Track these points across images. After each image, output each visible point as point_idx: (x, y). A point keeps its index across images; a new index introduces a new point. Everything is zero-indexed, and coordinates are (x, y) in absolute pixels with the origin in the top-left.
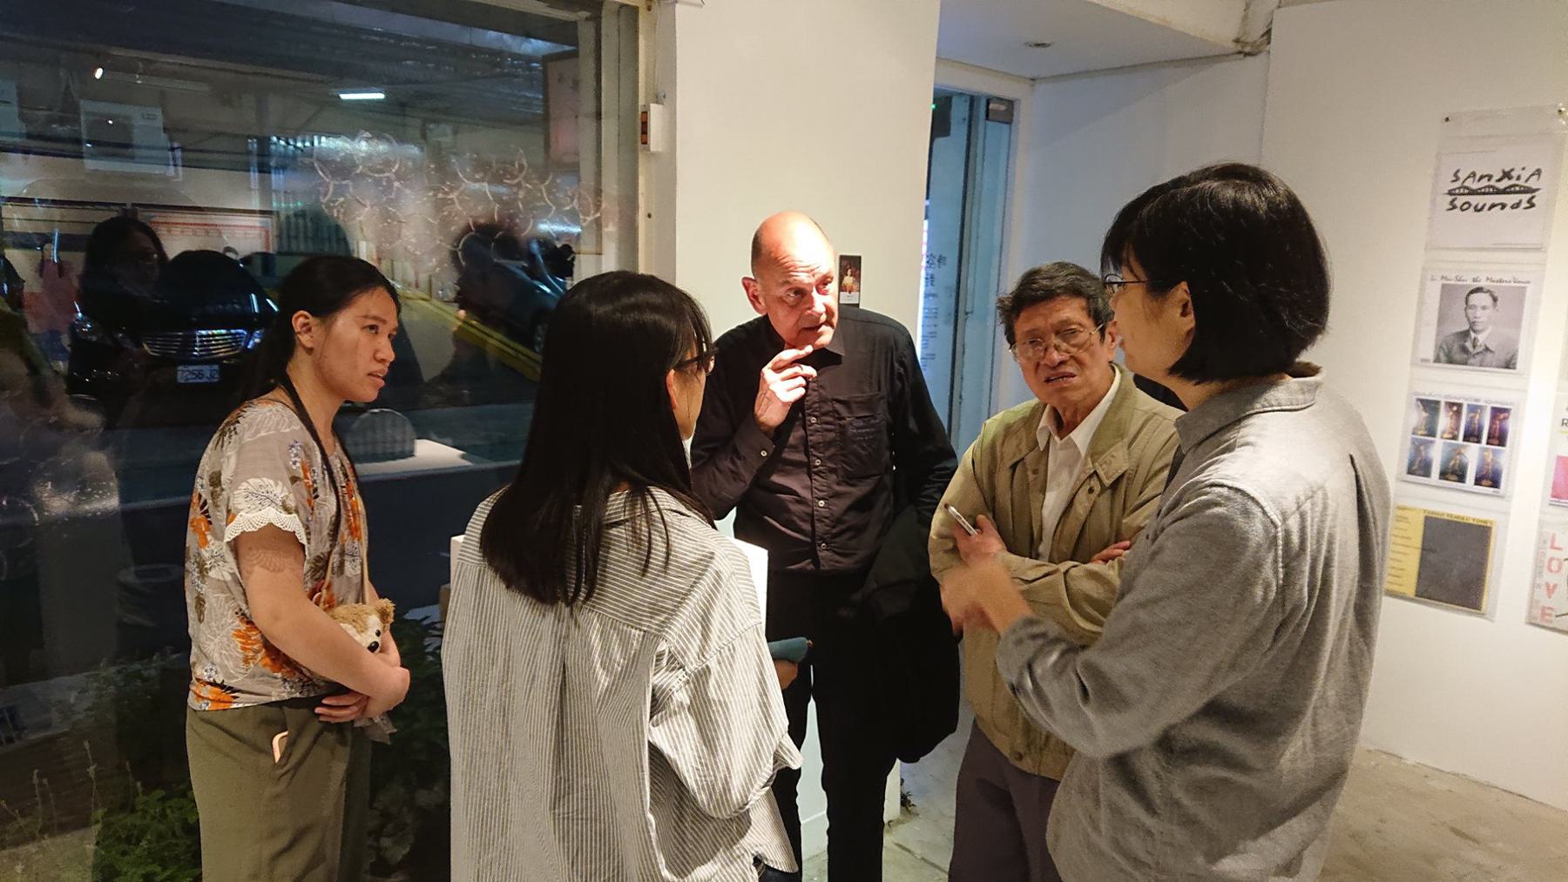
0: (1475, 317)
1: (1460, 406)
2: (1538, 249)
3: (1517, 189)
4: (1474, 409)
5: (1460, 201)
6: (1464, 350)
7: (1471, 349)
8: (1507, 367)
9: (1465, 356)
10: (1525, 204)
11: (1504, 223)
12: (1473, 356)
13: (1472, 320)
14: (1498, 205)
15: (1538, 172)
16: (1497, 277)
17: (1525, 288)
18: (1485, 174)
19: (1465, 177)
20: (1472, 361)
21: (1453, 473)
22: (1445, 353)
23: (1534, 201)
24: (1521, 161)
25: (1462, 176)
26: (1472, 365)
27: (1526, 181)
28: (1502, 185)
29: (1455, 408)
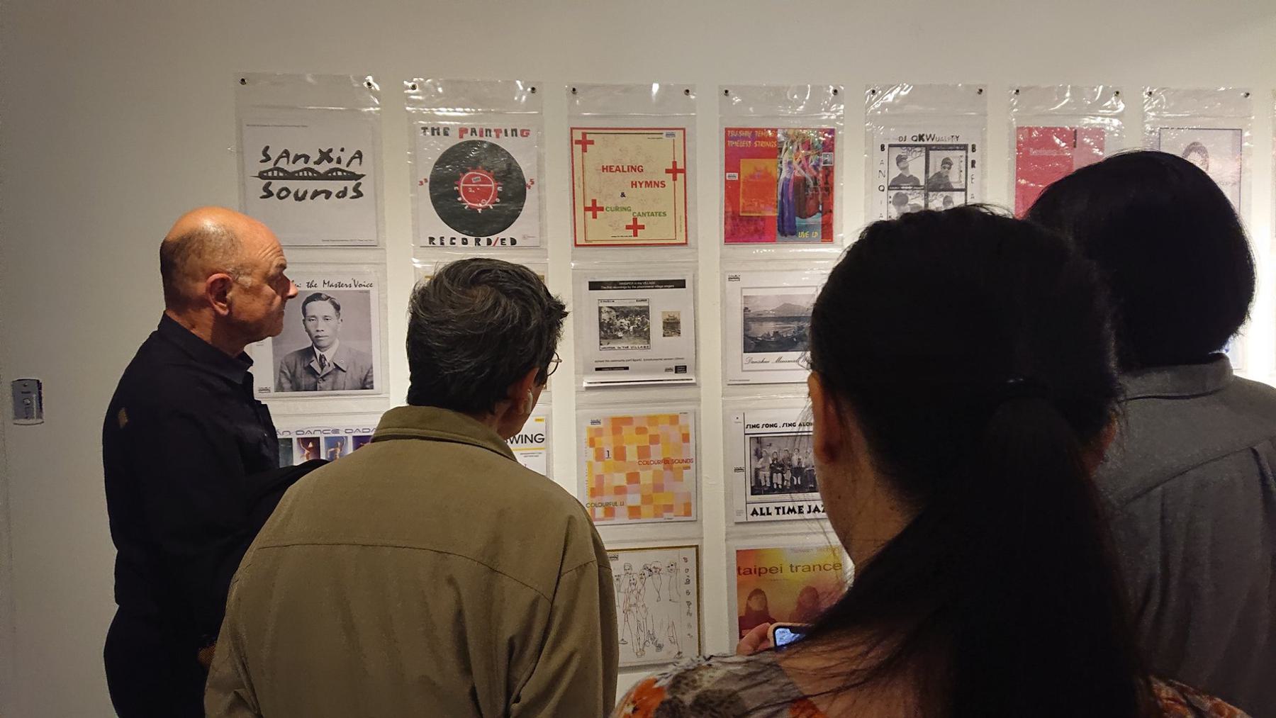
2: (373, 246)
3: (340, 173)
5: (276, 186)
6: (312, 372)
7: (319, 370)
9: (313, 380)
10: (351, 193)
12: (321, 378)
15: (359, 155)
17: (368, 292)
19: (276, 158)
20: (322, 384)
22: (288, 379)
24: (342, 142)
27: (348, 166)
28: (324, 167)
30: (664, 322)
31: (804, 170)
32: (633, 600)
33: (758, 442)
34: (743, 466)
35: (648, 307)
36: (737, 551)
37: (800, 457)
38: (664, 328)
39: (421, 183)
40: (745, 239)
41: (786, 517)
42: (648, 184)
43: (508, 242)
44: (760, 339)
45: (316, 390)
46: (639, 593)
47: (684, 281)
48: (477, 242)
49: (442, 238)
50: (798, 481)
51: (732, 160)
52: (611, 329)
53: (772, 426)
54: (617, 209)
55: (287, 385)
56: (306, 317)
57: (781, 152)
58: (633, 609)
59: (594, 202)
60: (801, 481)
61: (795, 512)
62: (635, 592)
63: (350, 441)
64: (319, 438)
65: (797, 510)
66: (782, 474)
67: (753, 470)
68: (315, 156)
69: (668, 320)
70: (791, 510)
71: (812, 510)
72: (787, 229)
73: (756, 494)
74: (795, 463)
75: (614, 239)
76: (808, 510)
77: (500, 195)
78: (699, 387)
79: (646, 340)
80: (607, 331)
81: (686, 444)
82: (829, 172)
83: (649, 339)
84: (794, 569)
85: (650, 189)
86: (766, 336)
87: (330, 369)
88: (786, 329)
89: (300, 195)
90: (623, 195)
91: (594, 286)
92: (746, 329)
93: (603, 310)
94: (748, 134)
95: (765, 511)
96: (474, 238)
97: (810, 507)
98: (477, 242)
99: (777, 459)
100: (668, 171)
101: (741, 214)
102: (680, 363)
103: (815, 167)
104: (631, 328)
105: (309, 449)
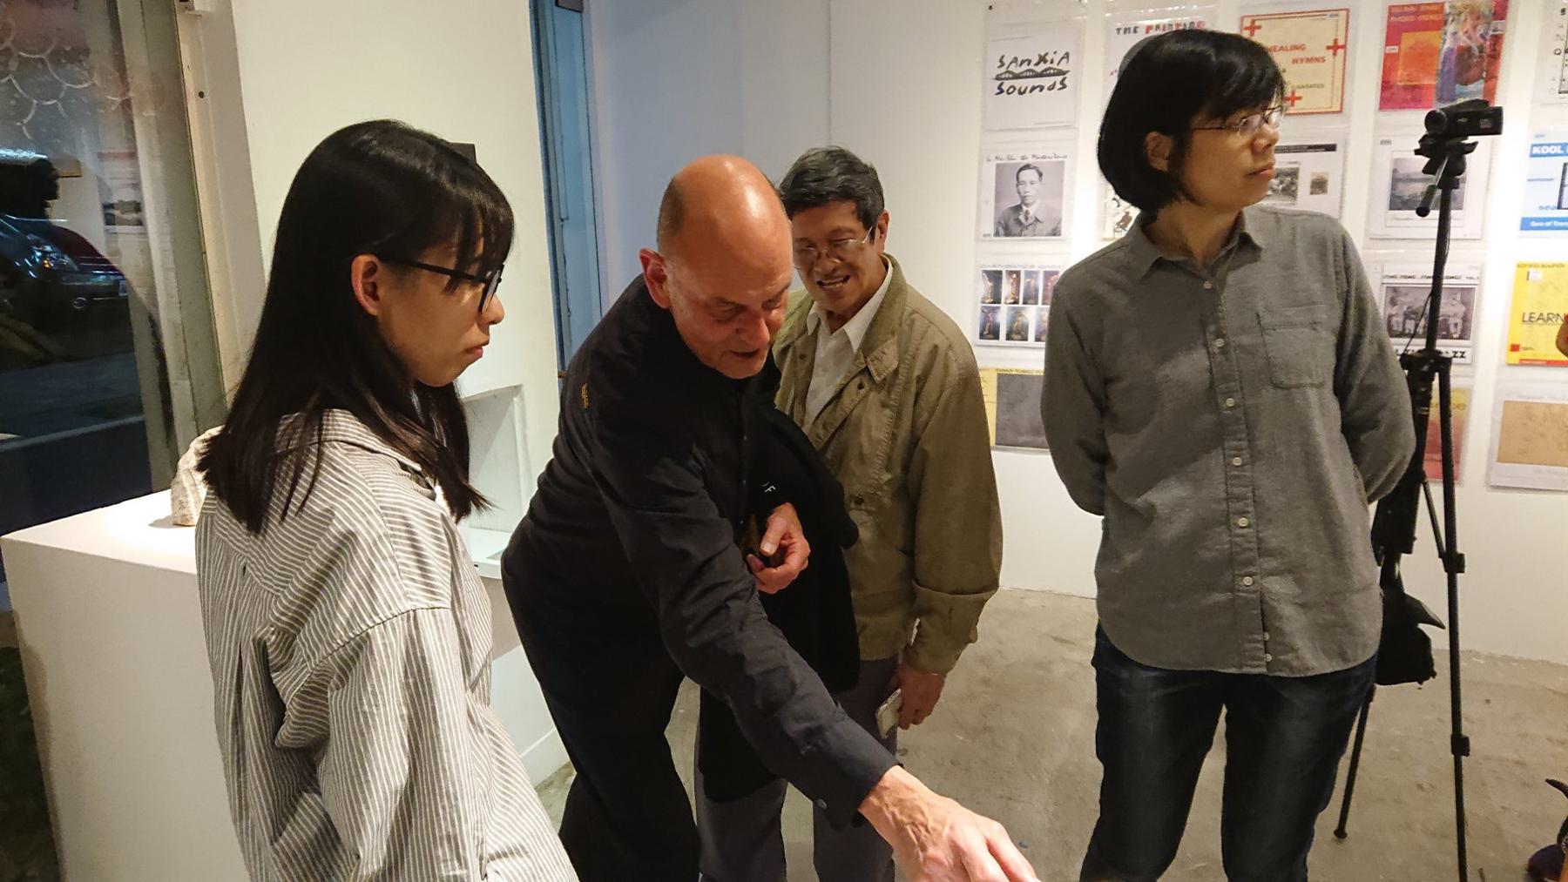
1: (1018, 273)
3: (1052, 71)
4: (1030, 274)
6: (1019, 222)
7: (1023, 220)
8: (1054, 235)
9: (1020, 228)
10: (1058, 86)
11: (1042, 103)
13: (1022, 194)
14: (1037, 87)
15: (1067, 56)
16: (1040, 155)
17: (1063, 162)
18: (1025, 58)
20: (1025, 232)
21: (1019, 333)
23: (1066, 82)
24: (1052, 45)
25: (1007, 61)
26: (1025, 235)
27: (1058, 64)
28: (1039, 69)
31: (1469, 38)
38: (1312, 187)
39: (1112, 74)
42: (1309, 60)
51: (1393, 36)
53: (1410, 277)
55: (1001, 231)
56: (1019, 182)
57: (1446, 24)
63: (1041, 277)
68: (1035, 60)
82: (1497, 40)
85: (1309, 65)
87: (1032, 221)
94: (1413, 9)
100: (1329, 48)
103: (1482, 36)
104: (1281, 186)
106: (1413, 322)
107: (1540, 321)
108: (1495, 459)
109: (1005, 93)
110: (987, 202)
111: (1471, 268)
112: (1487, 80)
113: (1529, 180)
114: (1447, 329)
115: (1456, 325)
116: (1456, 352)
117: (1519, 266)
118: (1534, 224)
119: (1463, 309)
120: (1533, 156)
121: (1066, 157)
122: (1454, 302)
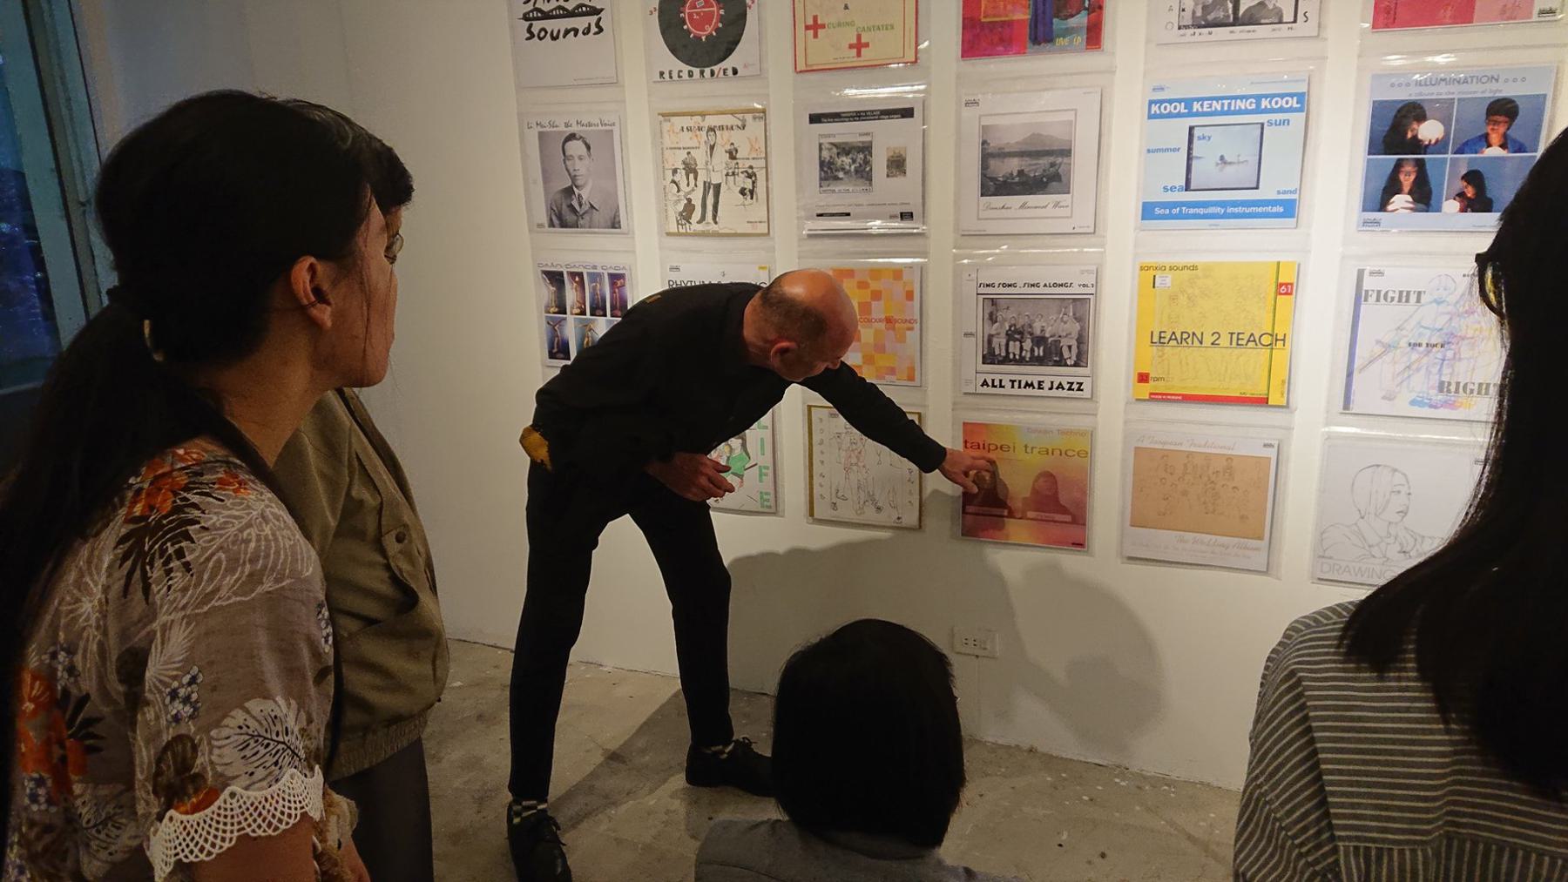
0: (575, 170)
1: (581, 275)
4: (595, 277)
5: (537, 25)
7: (577, 208)
8: (613, 227)
10: (594, 29)
12: (581, 216)
13: (572, 175)
17: (612, 131)
20: (581, 222)
22: (555, 214)
26: (581, 227)
29: (577, 276)
30: (888, 160)
32: (854, 460)
33: (993, 305)
34: (974, 331)
35: (871, 142)
36: (964, 423)
37: (1044, 325)
38: (888, 167)
39: (651, 13)
40: (987, 53)
41: (1023, 392)
43: (730, 72)
44: (1001, 179)
45: (578, 227)
46: (860, 453)
47: (912, 109)
48: (702, 73)
49: (670, 72)
50: (1039, 352)
52: (831, 169)
54: (839, 25)
55: (556, 221)
56: (566, 157)
58: (855, 468)
59: (815, 18)
60: (1044, 351)
61: (1034, 388)
62: (856, 452)
63: (606, 280)
64: (582, 273)
65: (1036, 385)
66: (1021, 342)
67: (986, 339)
69: (892, 157)
70: (1028, 385)
71: (1055, 385)
72: (1041, 35)
73: (988, 364)
74: (1038, 332)
75: (836, 61)
76: (1050, 386)
77: (721, 19)
78: (927, 238)
79: (868, 182)
80: (828, 172)
81: (909, 303)
83: (870, 179)
84: (1029, 450)
86: (1008, 175)
88: (1034, 167)
89: (555, 35)
90: (846, 7)
91: (815, 119)
92: (985, 166)
93: (823, 147)
95: (997, 383)
96: (698, 70)
97: (1052, 383)
98: (702, 73)
99: (1015, 325)
101: (983, 20)
102: (906, 209)
104: (853, 167)
105: (576, 282)
106: (1018, 343)
107: (1173, 343)
108: (1128, 523)
109: (536, 38)
110: (535, 182)
111: (1082, 272)
112: (1091, 10)
113: (1149, 151)
114: (1061, 355)
115: (1070, 347)
116: (1072, 383)
117: (1142, 268)
118: (1158, 211)
119: (1078, 326)
120: (1151, 117)
121: (614, 124)
122: (1065, 318)
